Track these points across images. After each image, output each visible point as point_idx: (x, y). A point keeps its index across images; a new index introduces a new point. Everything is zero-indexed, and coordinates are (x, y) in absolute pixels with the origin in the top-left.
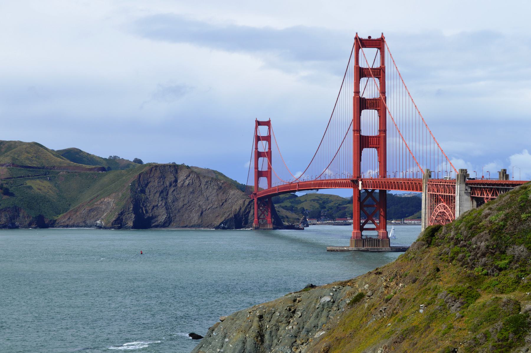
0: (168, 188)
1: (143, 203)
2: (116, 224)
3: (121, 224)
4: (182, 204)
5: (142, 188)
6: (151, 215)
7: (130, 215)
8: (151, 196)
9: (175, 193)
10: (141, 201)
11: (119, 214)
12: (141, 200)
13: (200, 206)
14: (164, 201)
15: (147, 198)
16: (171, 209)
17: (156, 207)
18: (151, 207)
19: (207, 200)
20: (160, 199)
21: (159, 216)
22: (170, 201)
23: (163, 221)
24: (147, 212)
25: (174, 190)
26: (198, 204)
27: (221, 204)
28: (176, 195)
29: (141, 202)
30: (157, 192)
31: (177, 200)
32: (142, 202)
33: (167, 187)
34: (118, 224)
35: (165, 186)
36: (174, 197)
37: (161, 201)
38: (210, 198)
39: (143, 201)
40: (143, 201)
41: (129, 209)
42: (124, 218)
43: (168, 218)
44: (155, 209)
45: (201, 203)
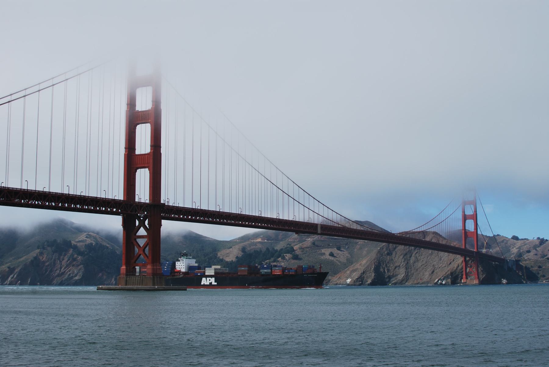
0: (412, 251)
1: (387, 264)
2: (358, 282)
3: (362, 282)
4: (421, 264)
5: (389, 252)
6: (392, 274)
7: (371, 274)
8: (396, 258)
9: (417, 255)
10: (384, 263)
11: (361, 273)
12: (385, 261)
13: (434, 265)
14: (406, 262)
15: (392, 260)
16: (411, 268)
17: (398, 267)
18: (393, 268)
19: (441, 259)
20: (403, 260)
21: (399, 274)
22: (412, 262)
23: (401, 278)
24: (388, 270)
25: (417, 252)
26: (433, 264)
27: (449, 263)
28: (418, 257)
29: (385, 263)
30: (401, 255)
31: (418, 261)
32: (386, 263)
33: (412, 250)
34: (360, 282)
35: (410, 249)
36: (416, 258)
37: (403, 262)
38: (443, 259)
39: (387, 262)
40: (387, 262)
41: (371, 269)
42: (365, 277)
43: (406, 276)
44: (397, 269)
45: (435, 263)
